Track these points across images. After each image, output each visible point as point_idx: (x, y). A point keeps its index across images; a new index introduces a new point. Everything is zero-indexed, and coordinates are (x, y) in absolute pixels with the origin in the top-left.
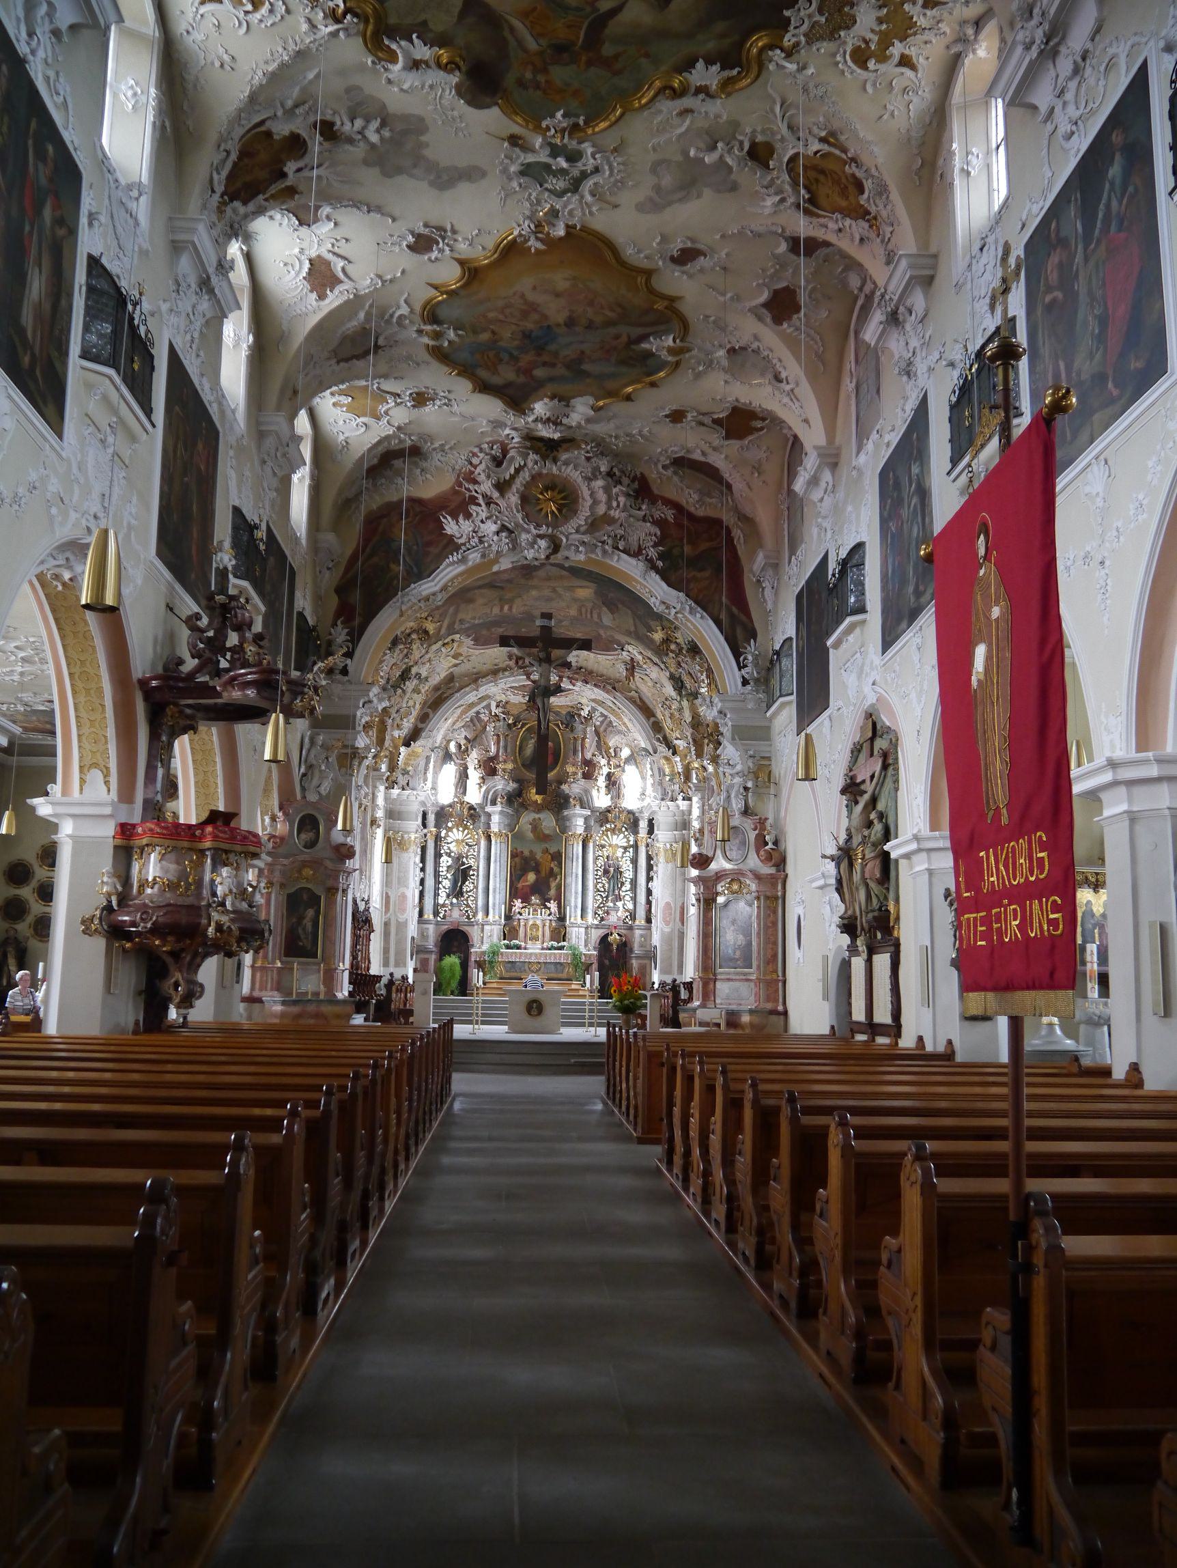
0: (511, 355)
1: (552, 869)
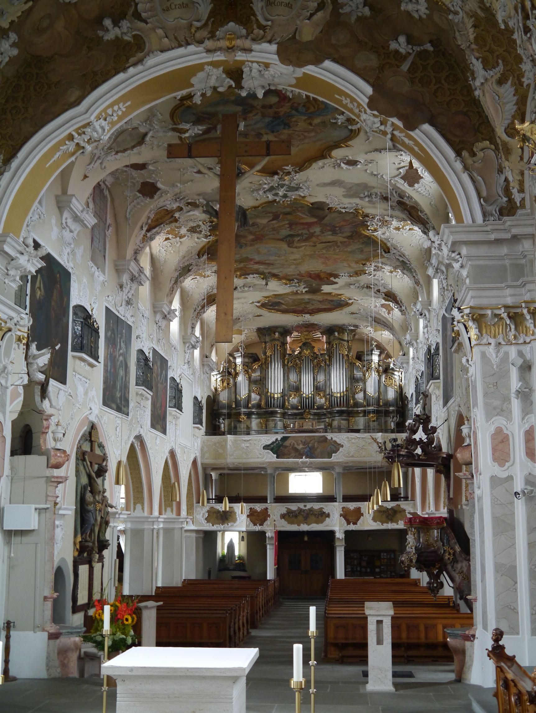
0: (297, 110)
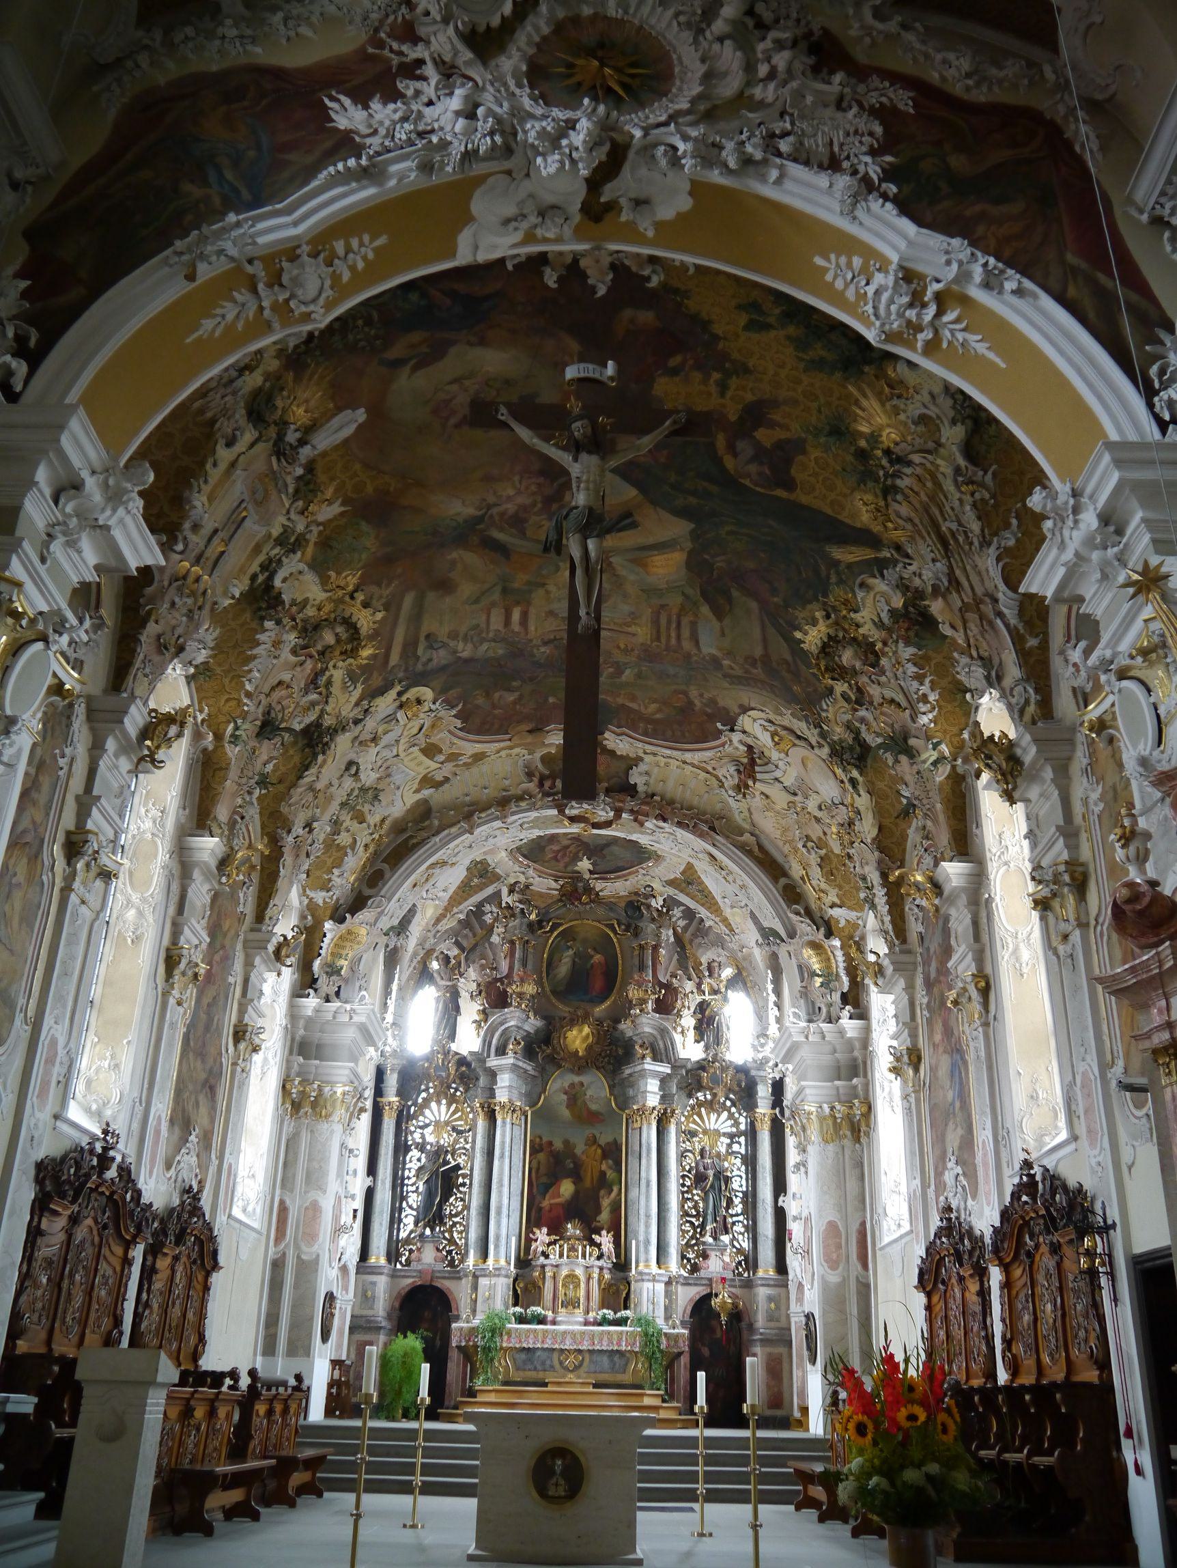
1: (603, 1174)
